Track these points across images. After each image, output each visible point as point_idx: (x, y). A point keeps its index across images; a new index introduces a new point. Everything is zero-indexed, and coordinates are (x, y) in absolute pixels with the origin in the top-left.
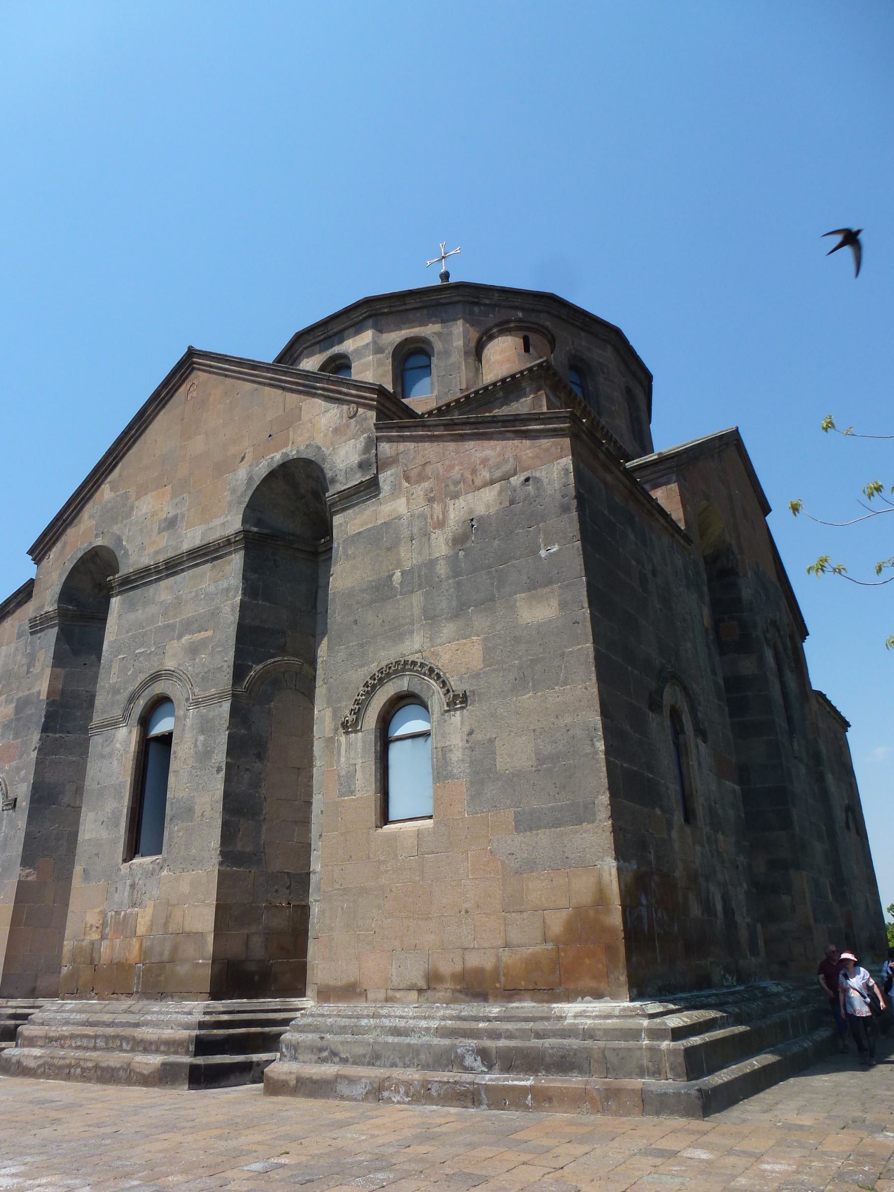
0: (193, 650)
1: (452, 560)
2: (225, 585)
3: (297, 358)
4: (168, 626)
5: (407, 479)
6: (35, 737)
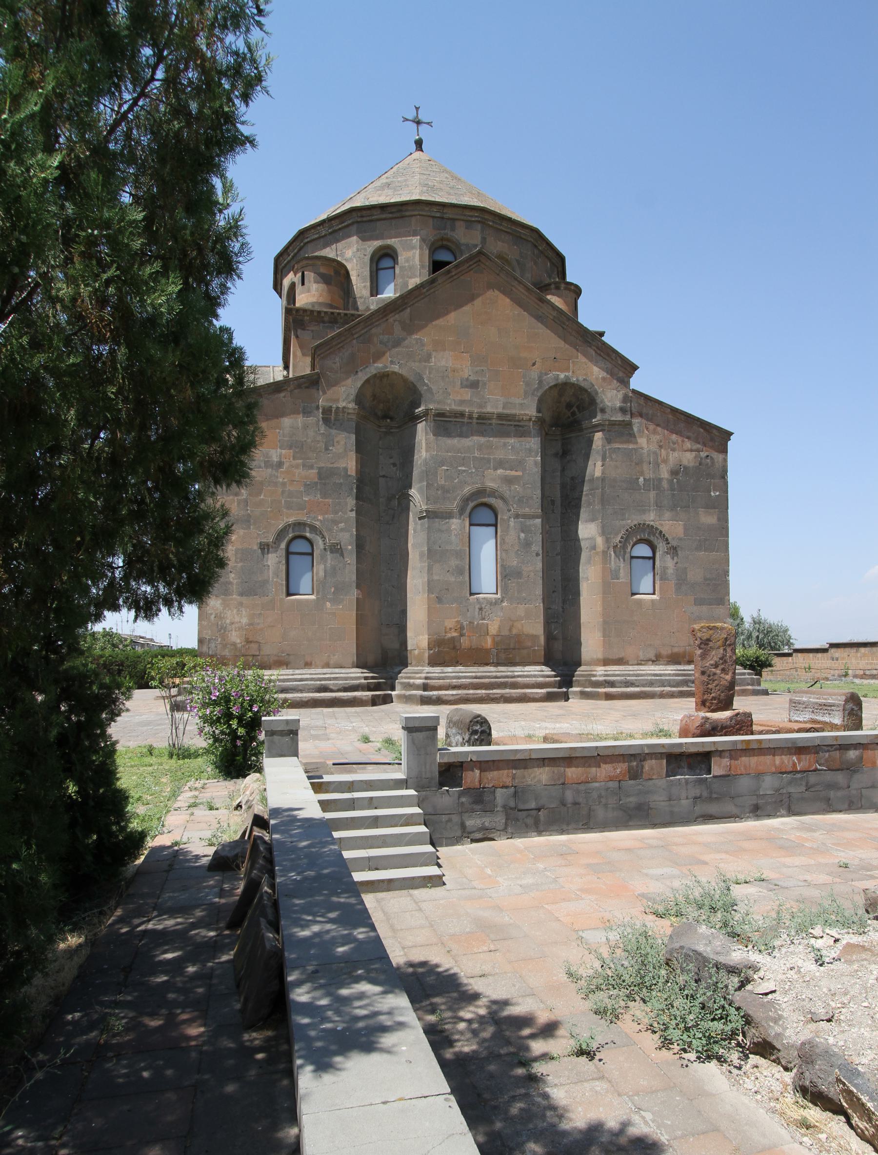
0: (509, 481)
1: (670, 482)
2: (528, 446)
3: (406, 216)
4: (484, 458)
5: (647, 429)
6: (351, 502)
